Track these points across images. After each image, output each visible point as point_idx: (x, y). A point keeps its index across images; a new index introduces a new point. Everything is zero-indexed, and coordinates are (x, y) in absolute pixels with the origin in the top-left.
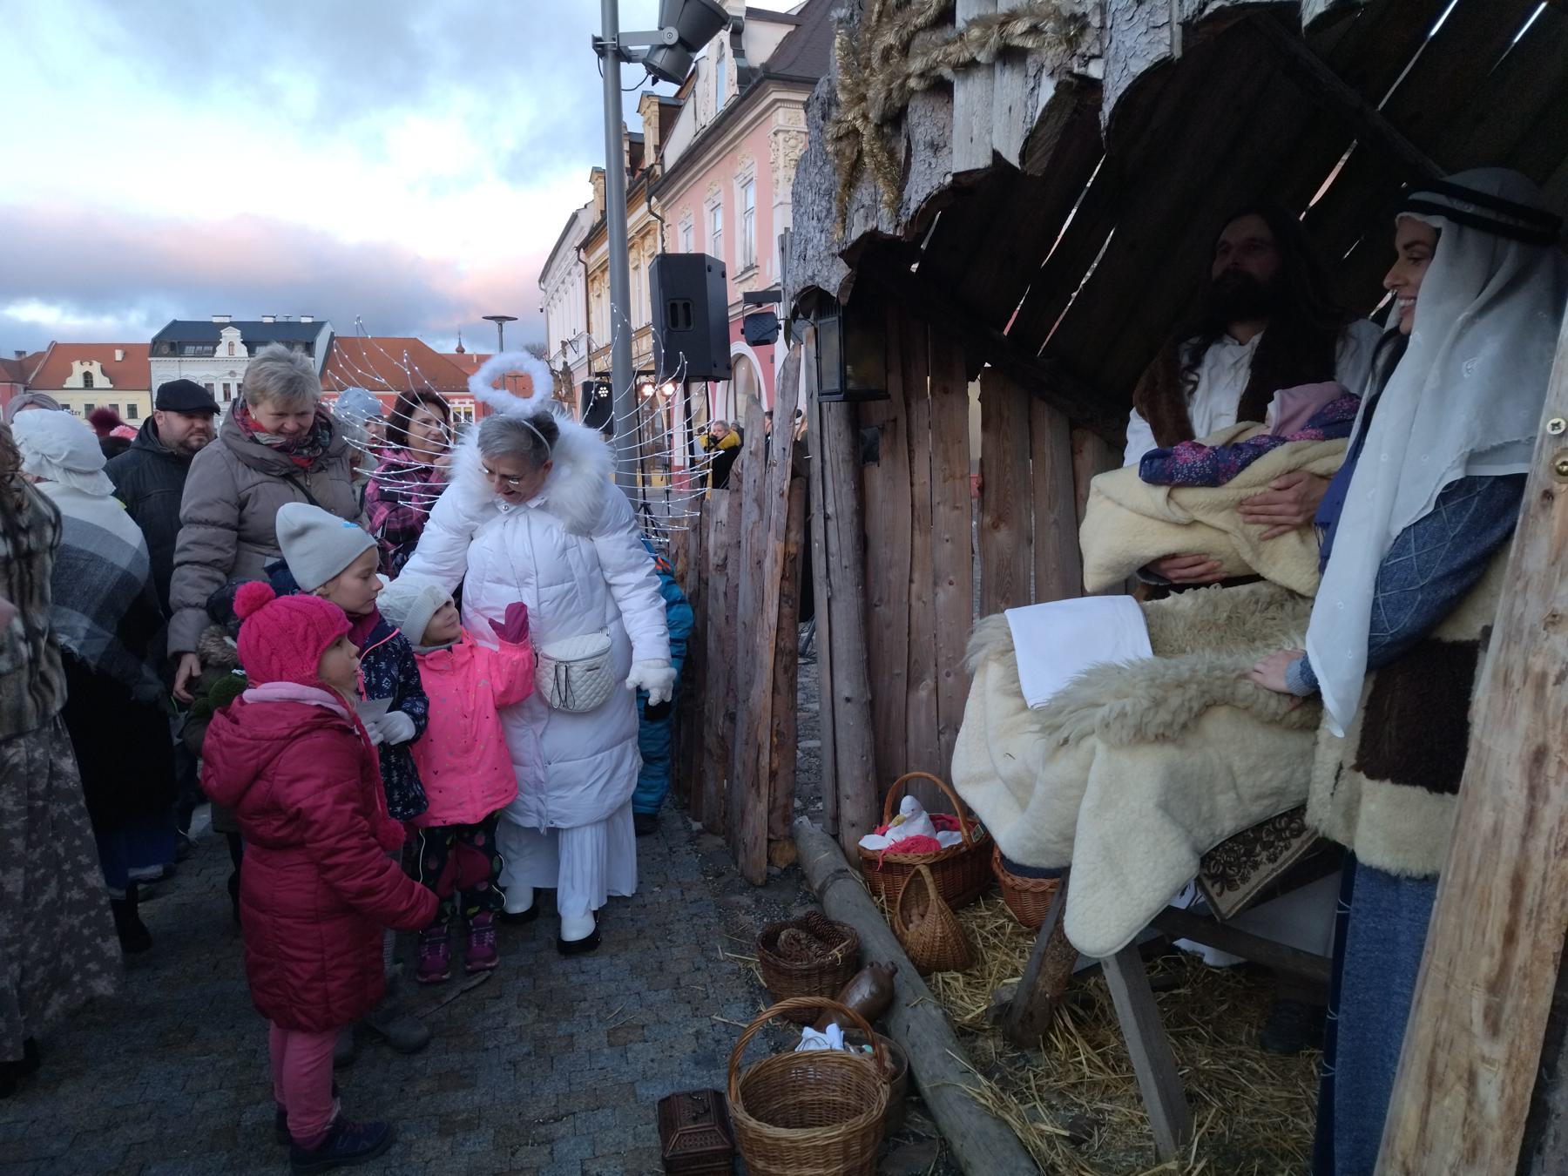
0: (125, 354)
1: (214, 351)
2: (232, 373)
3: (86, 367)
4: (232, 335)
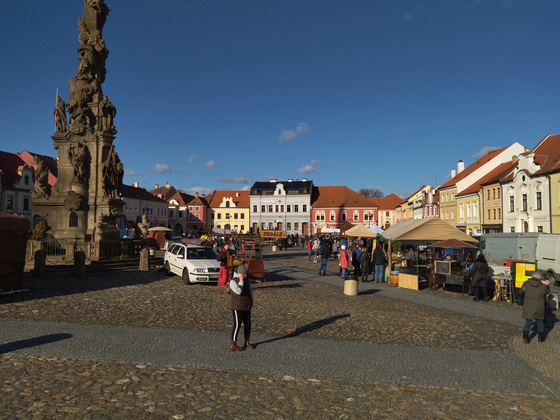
0: (239, 195)
1: (273, 193)
2: (280, 201)
3: (228, 199)
4: (280, 187)
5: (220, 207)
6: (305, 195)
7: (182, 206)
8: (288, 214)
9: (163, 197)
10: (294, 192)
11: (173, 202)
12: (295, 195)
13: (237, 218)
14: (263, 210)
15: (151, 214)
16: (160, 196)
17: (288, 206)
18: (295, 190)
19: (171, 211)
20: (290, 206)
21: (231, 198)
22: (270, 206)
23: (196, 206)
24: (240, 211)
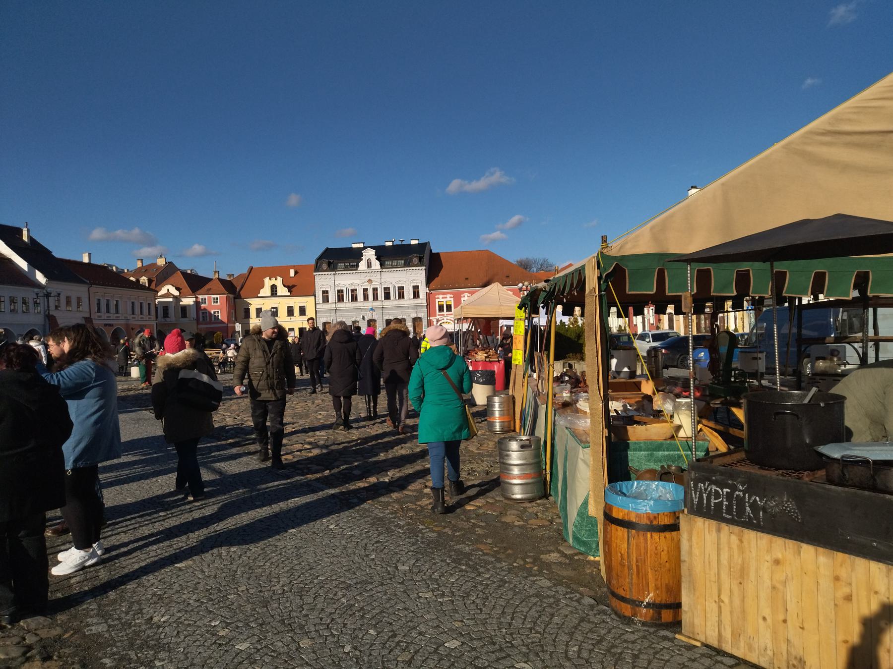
0: (296, 273)
1: (358, 266)
3: (273, 281)
4: (369, 254)
5: (259, 295)
6: (415, 268)
7: (186, 296)
8: (387, 303)
9: (150, 281)
10: (395, 263)
11: (168, 290)
12: (398, 269)
13: (292, 315)
14: (340, 299)
15: (117, 312)
16: (144, 280)
17: (385, 289)
18: (397, 260)
19: (166, 307)
20: (389, 288)
21: (280, 279)
22: (353, 291)
23: (213, 296)
24: (297, 302)
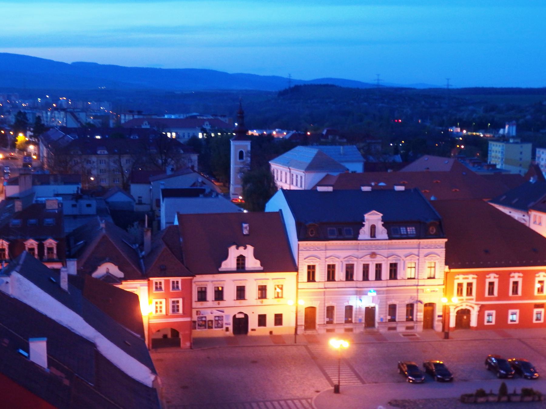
3: (241, 251)
5: (220, 270)
21: (250, 249)
